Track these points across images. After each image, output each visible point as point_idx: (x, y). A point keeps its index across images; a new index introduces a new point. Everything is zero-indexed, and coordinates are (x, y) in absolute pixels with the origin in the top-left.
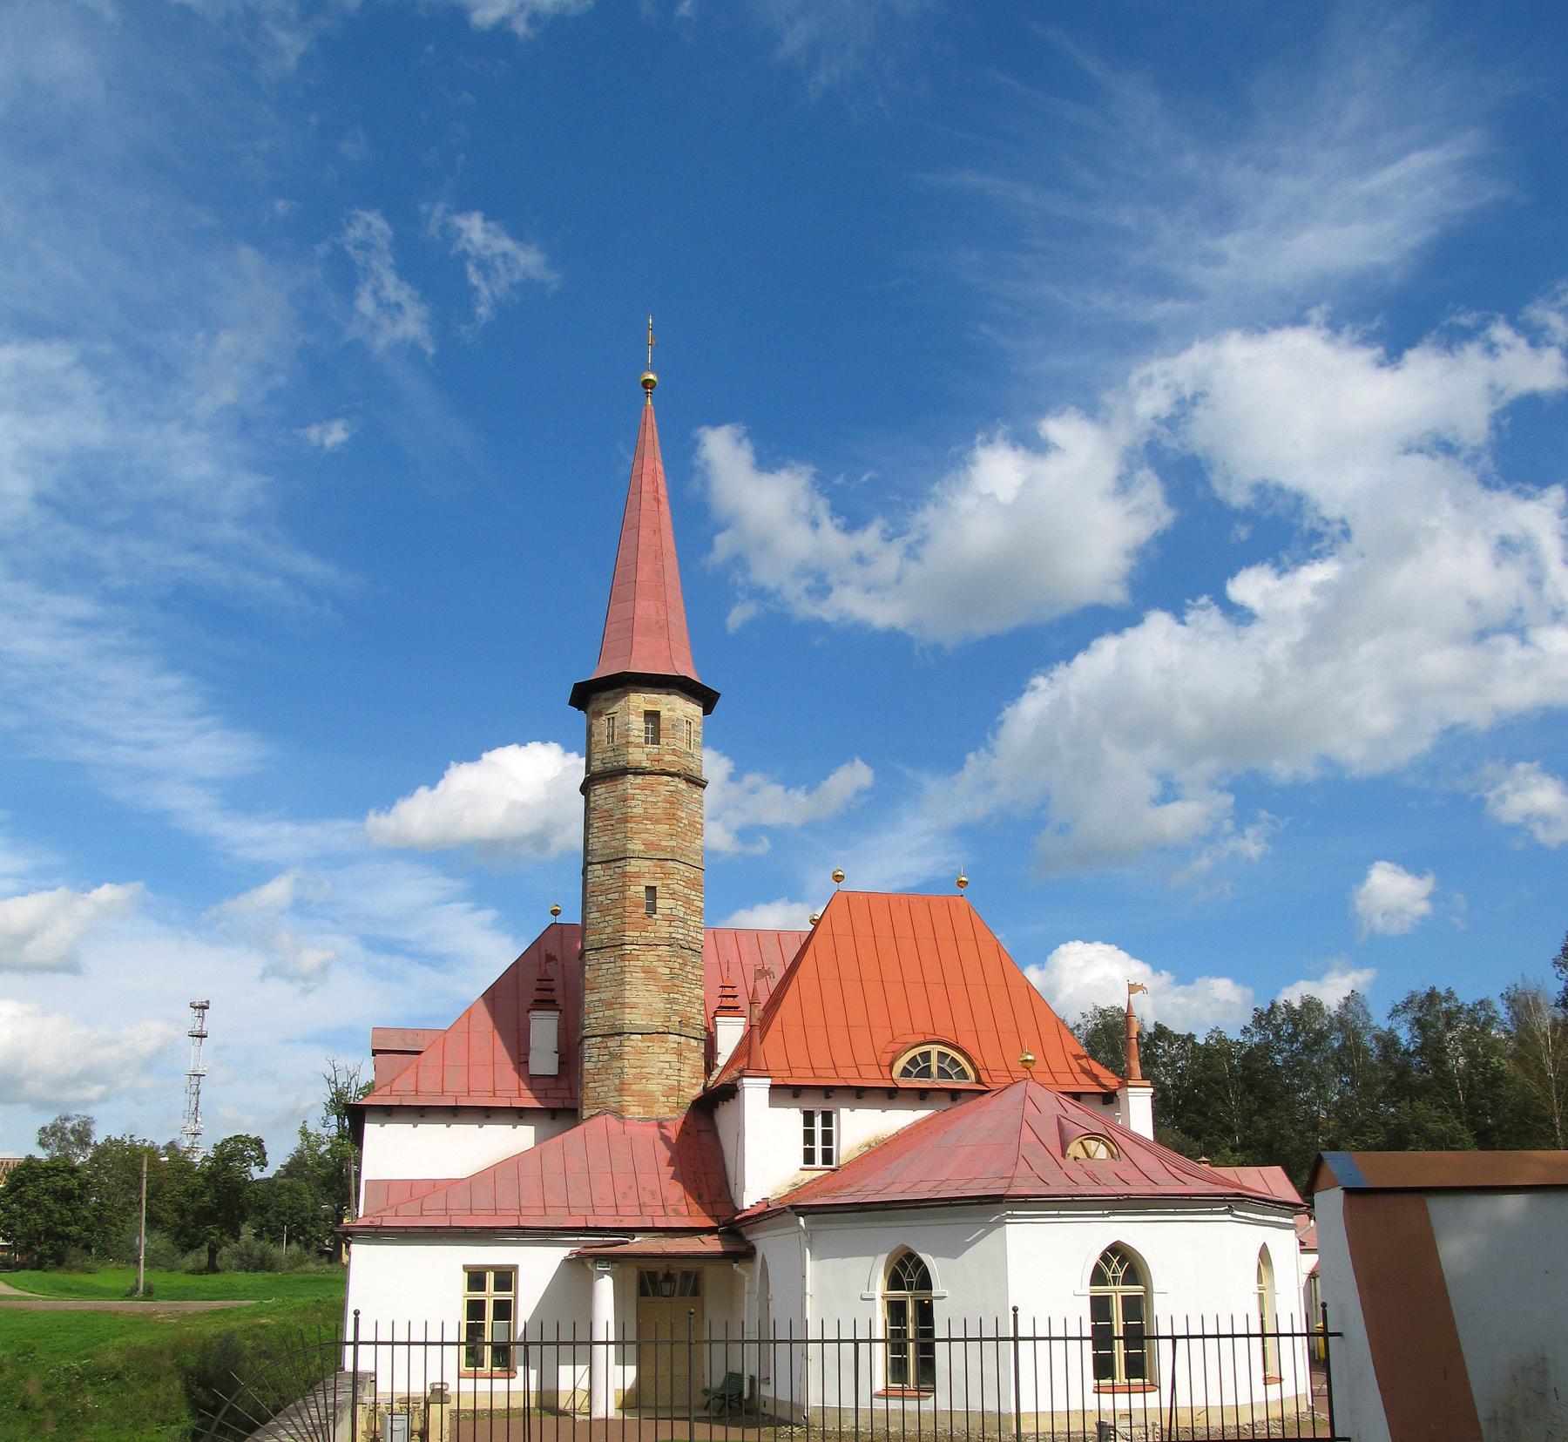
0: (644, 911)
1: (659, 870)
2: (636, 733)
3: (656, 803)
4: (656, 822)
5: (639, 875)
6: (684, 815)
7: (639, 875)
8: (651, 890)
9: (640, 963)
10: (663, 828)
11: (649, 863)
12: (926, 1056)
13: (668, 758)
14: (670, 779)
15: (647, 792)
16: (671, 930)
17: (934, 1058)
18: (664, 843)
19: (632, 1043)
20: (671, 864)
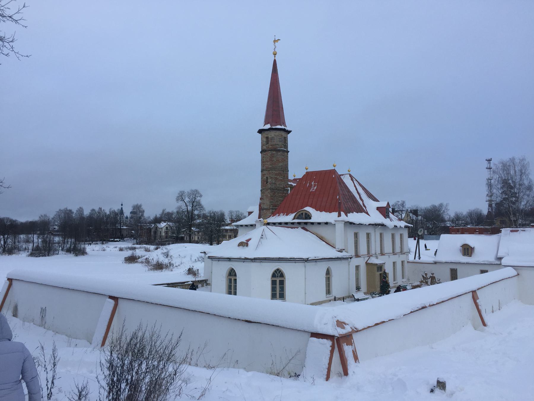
0: (266, 182)
1: (268, 173)
2: (264, 142)
3: (268, 158)
4: (267, 162)
5: (265, 175)
6: (275, 159)
7: (265, 175)
8: (267, 177)
9: (265, 194)
10: (269, 163)
11: (267, 171)
12: (302, 214)
13: (270, 147)
14: (270, 152)
15: (266, 156)
16: (271, 186)
17: (304, 214)
18: (269, 167)
19: (264, 212)
20: (270, 171)
